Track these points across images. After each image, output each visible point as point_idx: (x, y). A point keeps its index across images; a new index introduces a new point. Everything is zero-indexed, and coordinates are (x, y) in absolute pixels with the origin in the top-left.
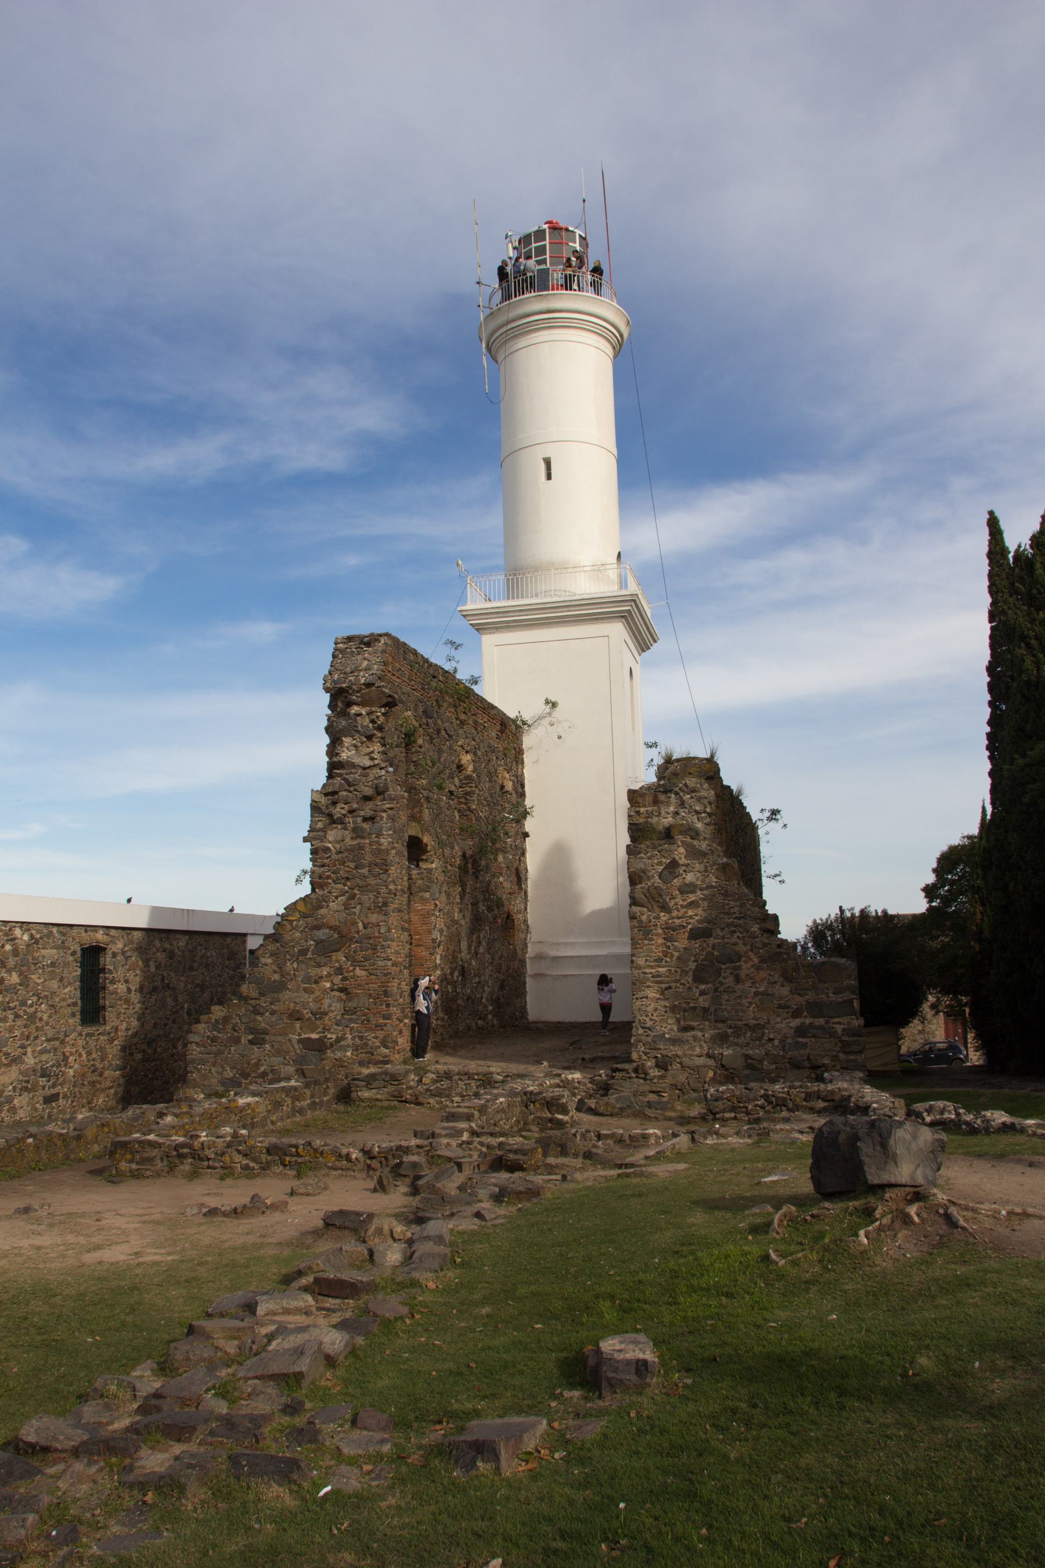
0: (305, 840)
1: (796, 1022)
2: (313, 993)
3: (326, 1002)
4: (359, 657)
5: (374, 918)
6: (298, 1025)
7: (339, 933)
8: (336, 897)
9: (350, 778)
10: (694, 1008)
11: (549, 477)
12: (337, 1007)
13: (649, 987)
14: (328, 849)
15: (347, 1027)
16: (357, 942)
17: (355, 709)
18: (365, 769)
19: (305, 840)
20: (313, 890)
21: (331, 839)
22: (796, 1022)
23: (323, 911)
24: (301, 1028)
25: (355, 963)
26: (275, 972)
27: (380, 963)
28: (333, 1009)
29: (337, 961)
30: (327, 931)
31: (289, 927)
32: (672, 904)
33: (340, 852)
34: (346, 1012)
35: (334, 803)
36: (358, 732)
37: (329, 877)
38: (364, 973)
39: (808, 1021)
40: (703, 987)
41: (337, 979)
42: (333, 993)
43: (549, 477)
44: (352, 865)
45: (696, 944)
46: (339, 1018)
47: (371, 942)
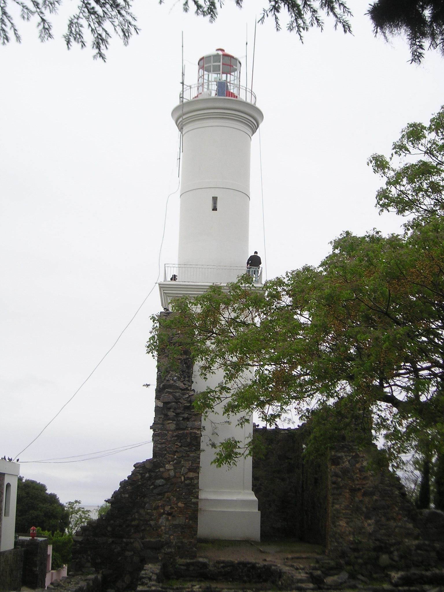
1: (416, 542)
3: (160, 521)
5: (191, 475)
10: (364, 533)
11: (215, 209)
13: (341, 520)
22: (416, 542)
23: (162, 469)
25: (179, 499)
27: (193, 500)
32: (355, 477)
38: (183, 505)
39: (422, 542)
40: (369, 521)
42: (164, 516)
43: (215, 209)
45: (367, 499)
46: (167, 530)
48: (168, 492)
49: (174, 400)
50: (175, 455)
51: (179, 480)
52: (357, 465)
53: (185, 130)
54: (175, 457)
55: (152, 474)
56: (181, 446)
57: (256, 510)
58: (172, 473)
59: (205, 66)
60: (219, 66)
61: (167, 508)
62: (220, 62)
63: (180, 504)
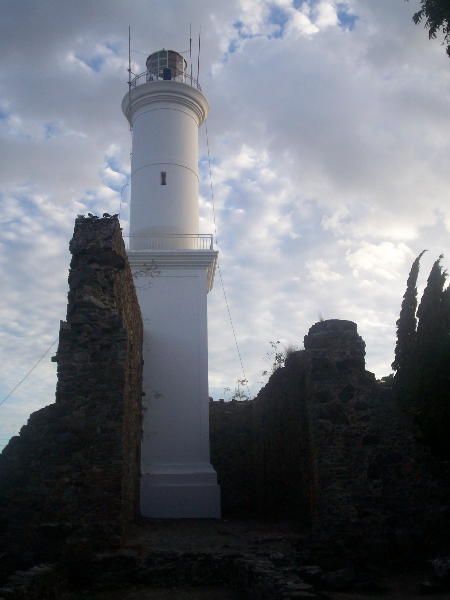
0: (54, 359)
4: (97, 232)
8: (79, 407)
9: (93, 314)
11: (164, 183)
17: (95, 266)
18: (100, 309)
19: (54, 359)
20: (58, 400)
32: (349, 418)
36: (98, 282)
40: (375, 481)
43: (164, 183)
50: (87, 397)
52: (351, 401)
53: (134, 117)
54: (88, 399)
57: (216, 484)
60: (166, 60)
62: (166, 57)
63: (95, 469)
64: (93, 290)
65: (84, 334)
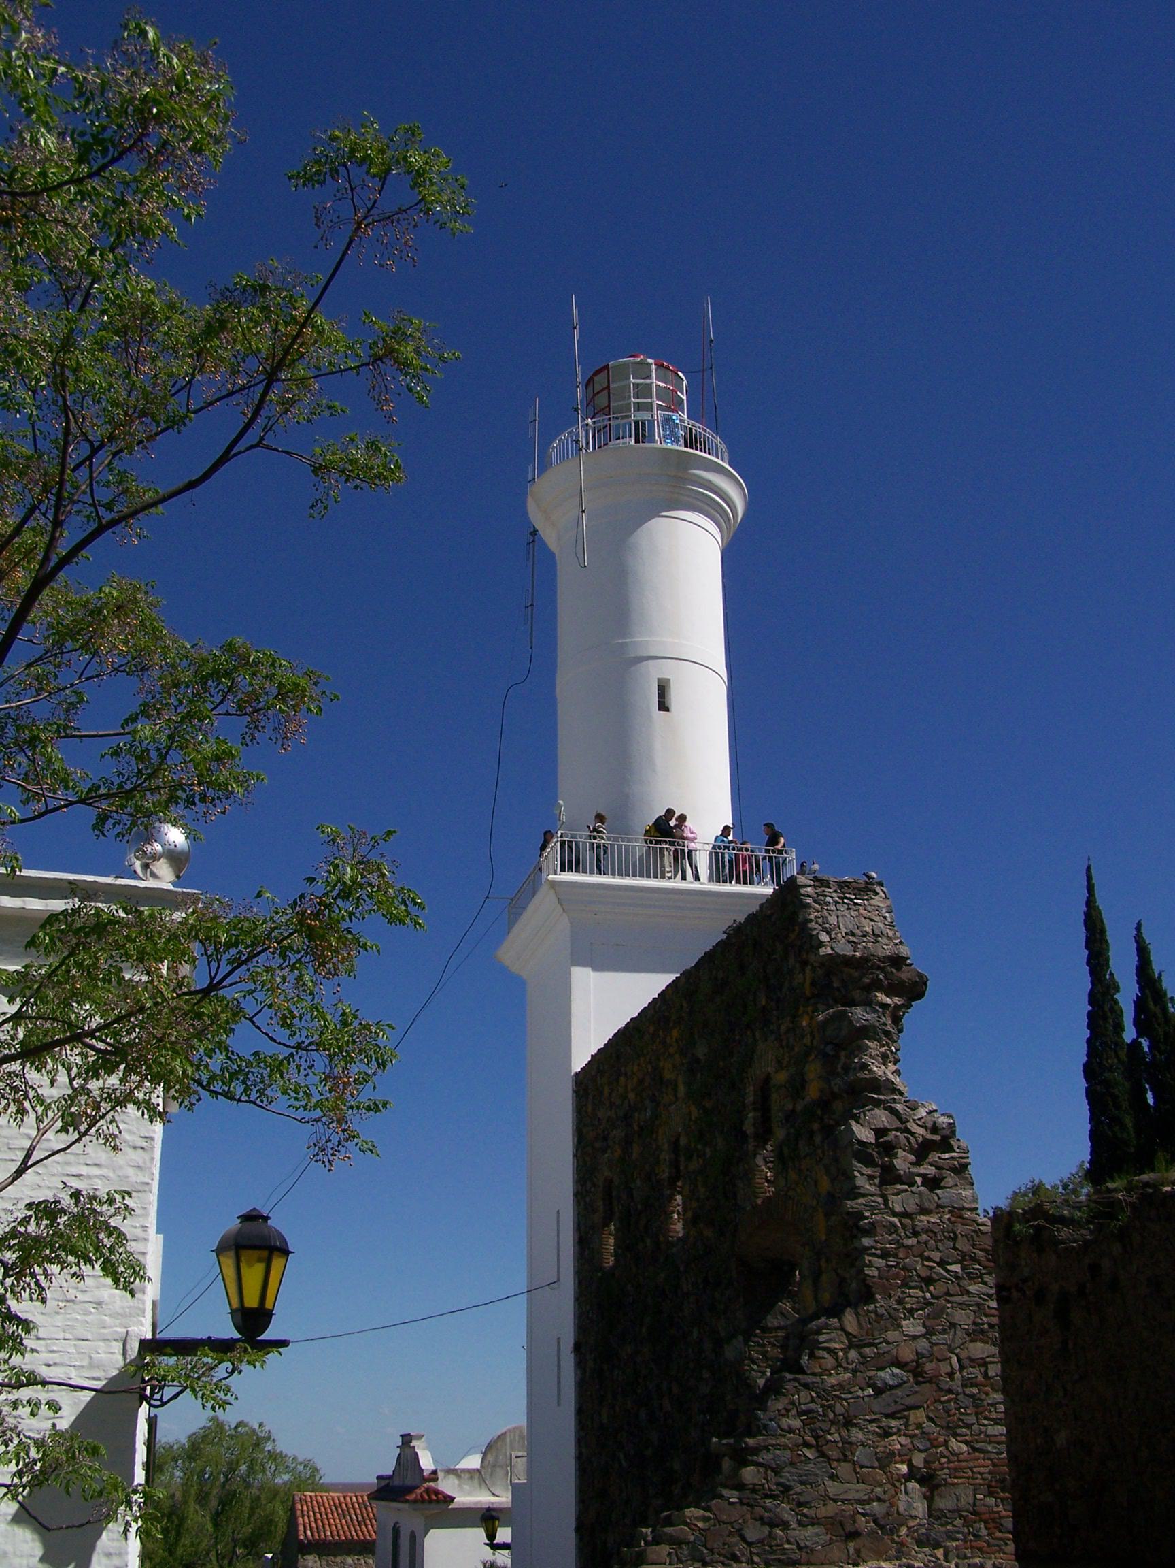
2: (880, 1485)
6: (851, 1545)
7: (917, 1372)
8: (911, 1311)
12: (920, 1508)
14: (895, 1226)
15: (937, 1545)
16: (950, 1391)
21: (898, 1209)
23: (891, 1335)
24: (858, 1551)
26: (807, 1445)
28: (914, 1513)
29: (919, 1426)
30: (896, 1371)
31: (829, 1361)
33: (915, 1234)
34: (934, 1514)
35: (889, 1149)
37: (897, 1276)
38: (965, 1448)
41: (919, 1460)
43: (663, 707)
44: (936, 1256)
47: (975, 1390)
48: (917, 1407)
49: (897, 1124)
51: (944, 1368)
55: (867, 1350)
56: (942, 1263)
58: (922, 1345)
59: (612, 386)
61: (919, 1460)
64: (883, 1050)
65: (900, 1153)
